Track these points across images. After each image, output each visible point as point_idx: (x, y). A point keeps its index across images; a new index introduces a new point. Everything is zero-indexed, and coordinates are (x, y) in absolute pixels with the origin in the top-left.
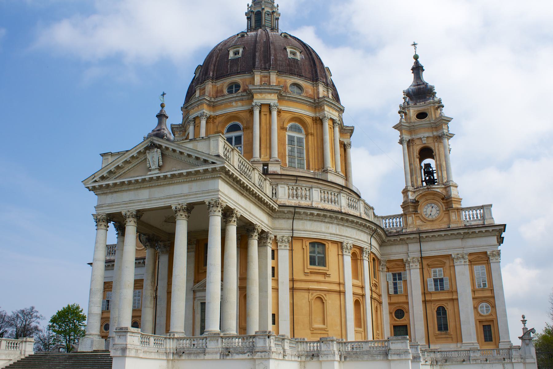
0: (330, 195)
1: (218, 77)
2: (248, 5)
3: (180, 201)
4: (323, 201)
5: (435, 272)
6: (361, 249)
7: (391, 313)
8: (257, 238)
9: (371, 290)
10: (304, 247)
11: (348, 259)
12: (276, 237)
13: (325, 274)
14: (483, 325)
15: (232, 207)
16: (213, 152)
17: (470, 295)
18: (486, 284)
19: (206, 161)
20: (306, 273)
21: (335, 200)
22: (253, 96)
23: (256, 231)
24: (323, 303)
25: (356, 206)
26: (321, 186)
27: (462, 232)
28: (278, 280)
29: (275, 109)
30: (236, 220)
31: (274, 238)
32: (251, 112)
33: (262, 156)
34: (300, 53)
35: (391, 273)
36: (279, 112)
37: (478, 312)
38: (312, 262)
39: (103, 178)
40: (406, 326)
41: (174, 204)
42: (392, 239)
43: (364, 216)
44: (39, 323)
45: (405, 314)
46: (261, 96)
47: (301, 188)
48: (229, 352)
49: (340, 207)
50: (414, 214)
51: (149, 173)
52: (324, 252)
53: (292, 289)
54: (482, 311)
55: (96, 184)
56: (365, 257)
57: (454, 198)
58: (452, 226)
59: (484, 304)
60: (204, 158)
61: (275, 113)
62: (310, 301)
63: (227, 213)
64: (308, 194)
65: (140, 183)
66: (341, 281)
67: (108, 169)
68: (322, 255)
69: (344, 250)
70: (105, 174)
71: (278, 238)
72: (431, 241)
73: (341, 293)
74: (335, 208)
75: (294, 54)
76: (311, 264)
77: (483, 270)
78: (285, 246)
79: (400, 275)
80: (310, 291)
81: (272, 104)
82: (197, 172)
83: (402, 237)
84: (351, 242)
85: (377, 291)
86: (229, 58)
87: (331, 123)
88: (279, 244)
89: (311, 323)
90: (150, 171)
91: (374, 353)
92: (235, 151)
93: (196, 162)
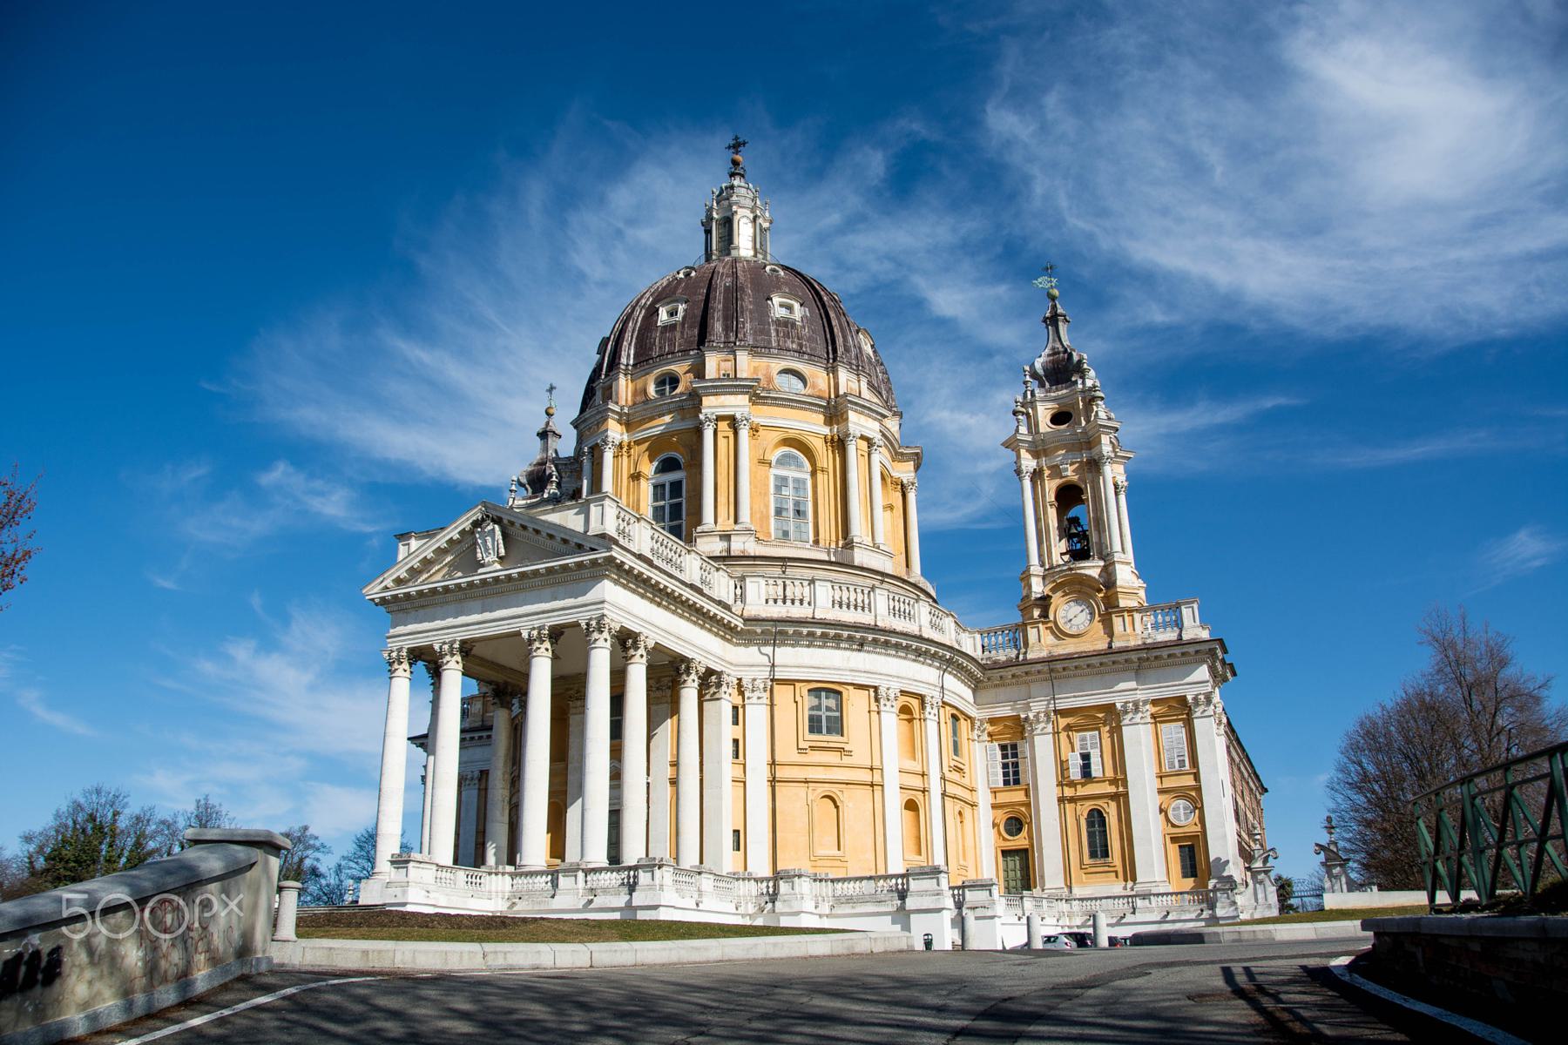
0: (852, 593)
3: (535, 622)
4: (837, 606)
5: (1083, 739)
6: (922, 699)
7: (995, 825)
8: (696, 684)
9: (943, 778)
10: (798, 698)
11: (891, 720)
12: (740, 680)
13: (841, 750)
14: (1180, 847)
15: (636, 629)
16: (595, 529)
17: (1156, 784)
18: (1184, 761)
19: (580, 548)
20: (801, 749)
22: (701, 400)
23: (694, 672)
24: (837, 807)
25: (912, 613)
26: (833, 576)
27: (1134, 656)
28: (744, 765)
29: (745, 425)
30: (645, 654)
31: (736, 682)
32: (699, 432)
33: (719, 520)
34: (801, 305)
35: (996, 744)
36: (755, 430)
37: (1168, 820)
38: (815, 725)
39: (399, 582)
40: (1026, 851)
42: (996, 674)
43: (928, 633)
44: (318, 860)
45: (1026, 827)
46: (717, 399)
47: (793, 582)
48: (595, 896)
49: (873, 618)
50: (1043, 623)
51: (480, 571)
52: (840, 708)
53: (773, 781)
54: (1177, 817)
56: (931, 713)
57: (1120, 587)
58: (1117, 644)
59: (1181, 803)
60: (575, 540)
61: (744, 433)
62: (809, 803)
63: (625, 641)
65: (465, 589)
66: (876, 764)
67: (407, 564)
68: (838, 714)
69: (882, 702)
71: (744, 683)
72: (1075, 676)
74: (865, 618)
75: (790, 308)
76: (812, 730)
77: (1178, 733)
78: (759, 698)
79: (1014, 747)
80: (810, 784)
81: (738, 416)
82: (565, 568)
83: (1014, 670)
84: (896, 686)
85: (966, 782)
86: (659, 324)
87: (864, 445)
88: (747, 694)
89: (811, 846)
90: (483, 566)
91: (883, 899)
93: (563, 547)
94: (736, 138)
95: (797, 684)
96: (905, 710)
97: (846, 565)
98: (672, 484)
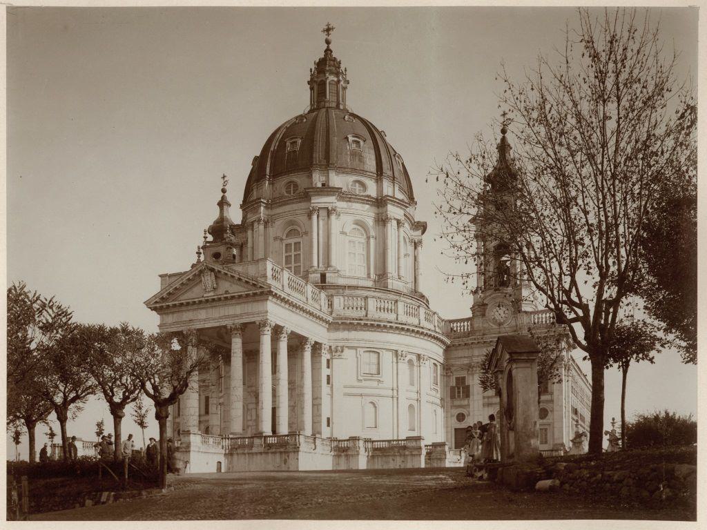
1: (276, 175)
2: (311, 69)
12: (330, 347)
21: (391, 309)
34: (364, 141)
39: (162, 298)
41: (228, 323)
55: (158, 305)
63: (277, 331)
64: (363, 304)
69: (399, 358)
70: (165, 295)
71: (333, 348)
73: (395, 398)
74: (392, 317)
81: (330, 208)
92: (284, 271)
94: (328, 25)
95: (358, 349)
96: (410, 361)
97: (385, 289)
98: (295, 243)
